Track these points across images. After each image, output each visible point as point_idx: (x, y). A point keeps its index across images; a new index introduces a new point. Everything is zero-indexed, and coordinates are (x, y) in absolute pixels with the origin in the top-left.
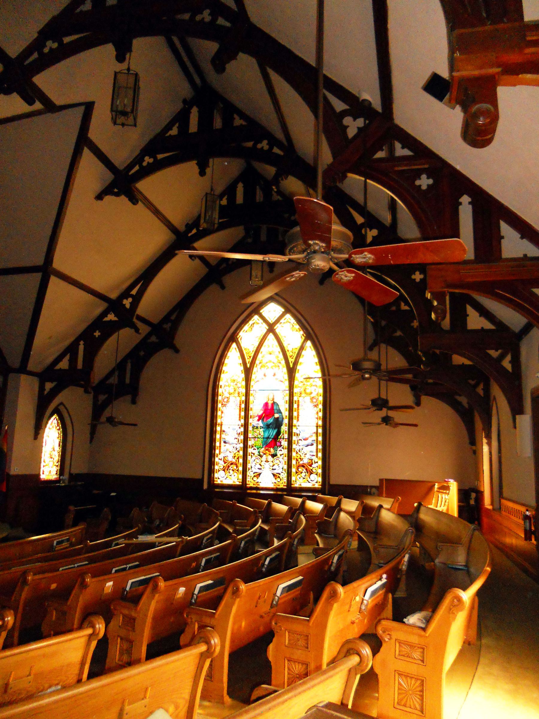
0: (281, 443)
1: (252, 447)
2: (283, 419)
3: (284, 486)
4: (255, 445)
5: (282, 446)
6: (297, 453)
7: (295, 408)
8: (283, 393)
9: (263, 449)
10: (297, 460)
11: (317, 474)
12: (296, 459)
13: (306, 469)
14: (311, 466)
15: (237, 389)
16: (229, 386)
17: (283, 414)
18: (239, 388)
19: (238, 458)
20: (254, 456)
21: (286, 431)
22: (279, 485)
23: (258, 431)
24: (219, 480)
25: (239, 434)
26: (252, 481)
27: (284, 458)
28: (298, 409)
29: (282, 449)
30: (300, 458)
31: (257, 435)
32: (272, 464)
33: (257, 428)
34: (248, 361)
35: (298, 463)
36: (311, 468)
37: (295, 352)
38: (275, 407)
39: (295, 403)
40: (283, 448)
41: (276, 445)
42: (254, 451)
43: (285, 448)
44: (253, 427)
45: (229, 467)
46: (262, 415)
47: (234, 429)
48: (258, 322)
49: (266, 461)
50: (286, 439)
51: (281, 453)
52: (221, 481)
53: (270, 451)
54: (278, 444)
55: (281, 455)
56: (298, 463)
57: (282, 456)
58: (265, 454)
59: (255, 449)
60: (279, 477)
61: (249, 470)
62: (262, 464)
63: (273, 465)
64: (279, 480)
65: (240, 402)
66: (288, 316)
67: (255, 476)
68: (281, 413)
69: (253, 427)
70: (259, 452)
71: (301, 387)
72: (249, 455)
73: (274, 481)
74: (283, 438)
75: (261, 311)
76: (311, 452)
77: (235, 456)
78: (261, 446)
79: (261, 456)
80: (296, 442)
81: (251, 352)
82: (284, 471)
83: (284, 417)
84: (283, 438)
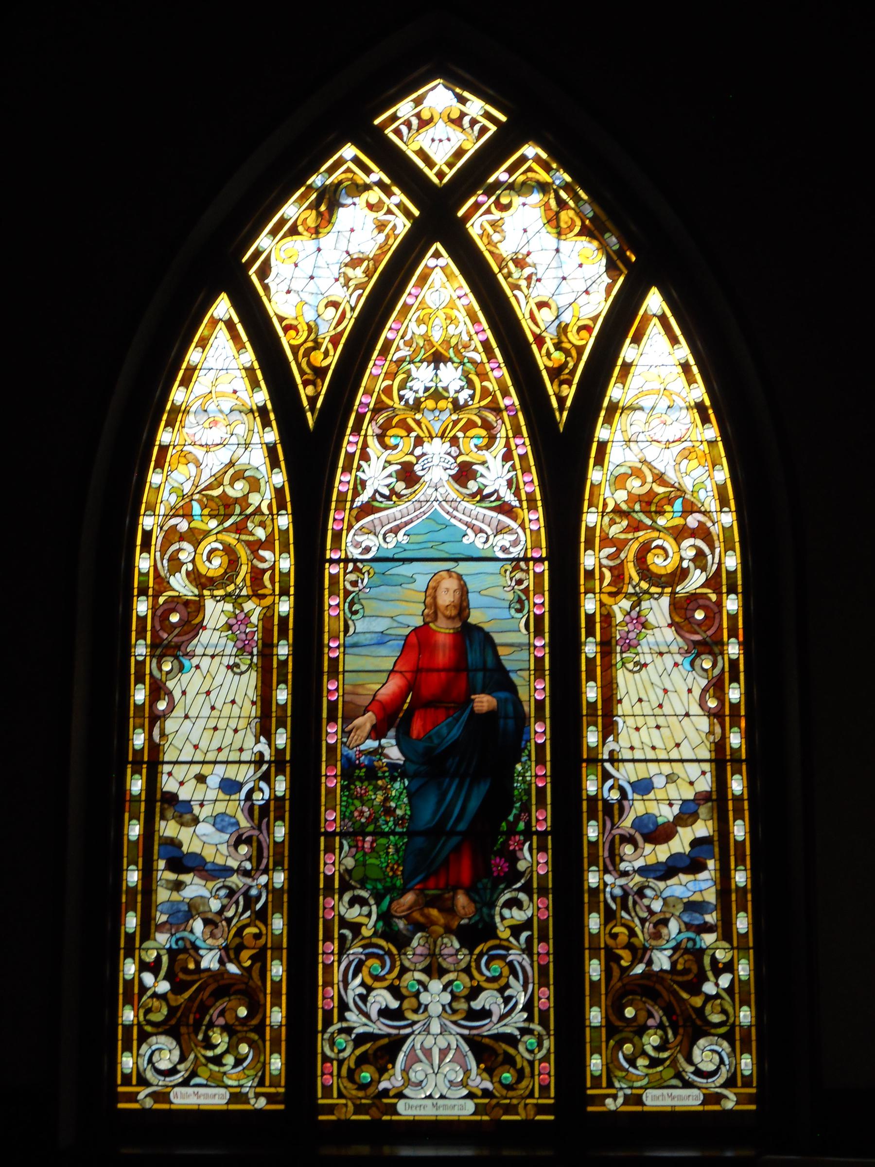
0: (514, 859)
1: (345, 887)
2: (522, 721)
3: (541, 1109)
4: (358, 874)
5: (520, 875)
6: (609, 916)
7: (591, 662)
8: (519, 575)
9: (409, 898)
10: (612, 958)
11: (729, 1037)
12: (608, 950)
13: (668, 1010)
14: (695, 988)
15: (243, 553)
16: (195, 537)
17: (523, 694)
18: (255, 547)
19: (260, 958)
20: (358, 943)
21: (541, 791)
22: (510, 1109)
23: (380, 797)
24: (143, 1093)
25: (264, 809)
26: (351, 1089)
27: (539, 948)
28: (608, 667)
29: (522, 896)
30: (630, 946)
31: (372, 819)
32: (462, 984)
33: (372, 774)
34: (399, 625)
35: (616, 973)
36: (698, 1001)
37: (580, 350)
38: (473, 657)
39: (590, 633)
40: (527, 889)
41: (488, 872)
42: (353, 914)
43: (543, 891)
44: (350, 770)
45: (204, 1009)
46: (400, 697)
47: (229, 786)
48: (361, 177)
49: (427, 971)
50: (542, 835)
51: (518, 916)
52: (161, 1096)
53: (449, 910)
54: (499, 865)
55: (516, 930)
56: (616, 973)
57: (524, 935)
58: (420, 927)
59: (363, 902)
60: (510, 1061)
61: (328, 1022)
62: (409, 981)
63: (475, 992)
64: (508, 1077)
65: (267, 631)
66: (655, 861)
67: (362, 1060)
68: (512, 688)
69: (350, 770)
70: (385, 917)
71: (620, 545)
72: (328, 937)
73: (480, 1082)
74: (528, 833)
75: (409, 225)
76: (693, 907)
77: (240, 947)
78: (399, 883)
79: (402, 942)
80: (603, 853)
81: (326, 344)
82: (537, 1027)
83: (530, 709)
84: (528, 833)
